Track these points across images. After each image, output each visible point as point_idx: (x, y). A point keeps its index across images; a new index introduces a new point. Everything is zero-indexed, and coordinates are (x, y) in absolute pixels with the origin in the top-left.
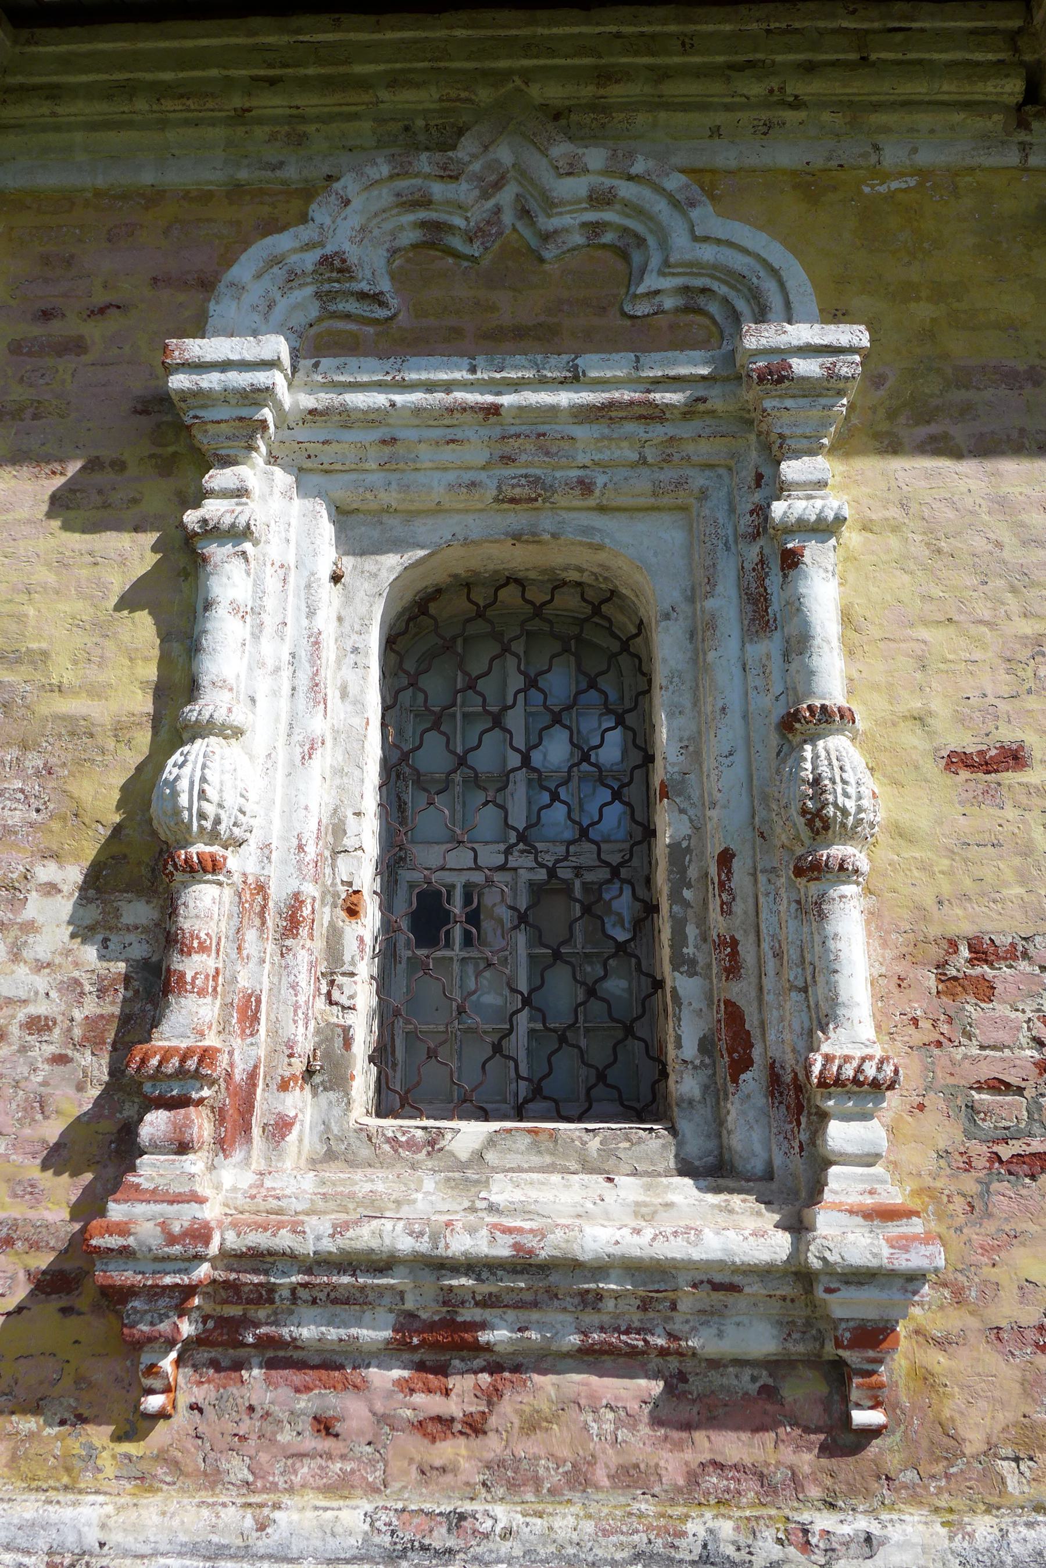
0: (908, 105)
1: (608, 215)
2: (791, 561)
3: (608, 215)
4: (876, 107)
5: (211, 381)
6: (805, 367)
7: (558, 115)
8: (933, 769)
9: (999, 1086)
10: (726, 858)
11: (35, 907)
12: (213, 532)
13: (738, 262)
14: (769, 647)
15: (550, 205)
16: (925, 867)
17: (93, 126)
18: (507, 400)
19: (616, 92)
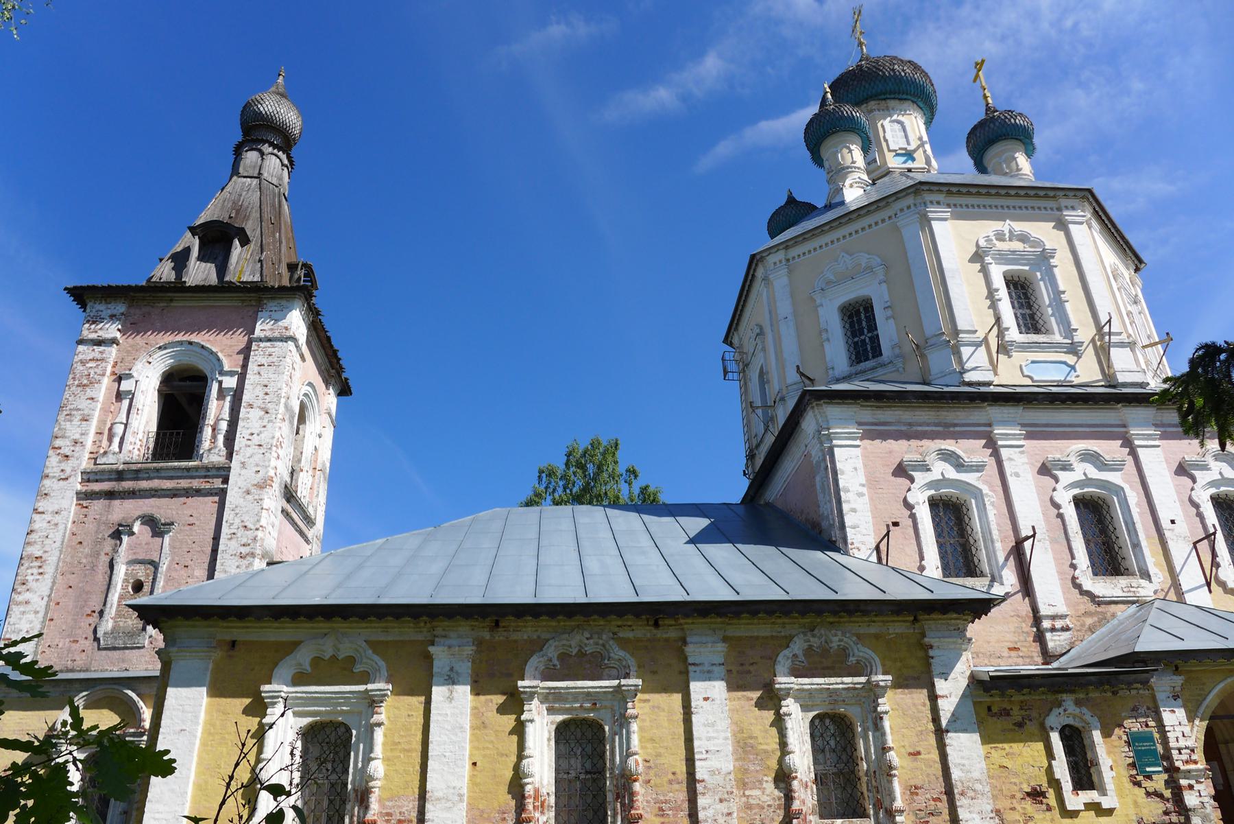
0: (893, 621)
1: (842, 643)
2: (881, 718)
3: (842, 643)
4: (888, 622)
5: (783, 686)
6: (882, 684)
7: (831, 623)
8: (906, 756)
9: (920, 810)
10: (875, 772)
11: (765, 785)
12: (786, 715)
13: (867, 656)
14: (878, 734)
15: (832, 642)
16: (906, 773)
17: (748, 624)
18: (831, 687)
19: (842, 620)
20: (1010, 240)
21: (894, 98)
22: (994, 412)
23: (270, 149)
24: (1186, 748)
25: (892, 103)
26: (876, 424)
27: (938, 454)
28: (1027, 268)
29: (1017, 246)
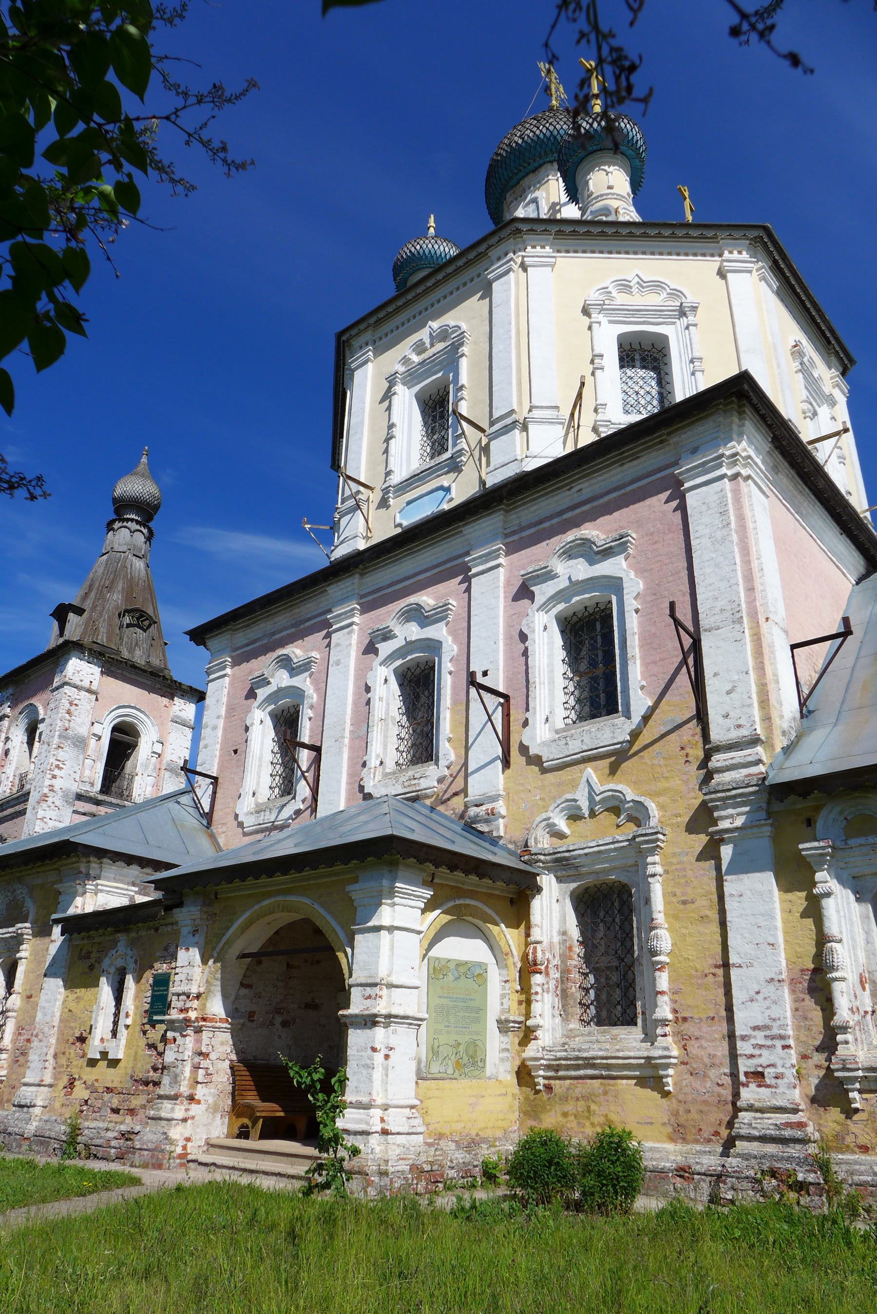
6: (19, 931)
20: (432, 345)
21: (527, 174)
22: (334, 590)
23: (120, 524)
24: (184, 994)
25: (526, 181)
26: (248, 645)
27: (277, 662)
28: (440, 375)
29: (440, 346)
